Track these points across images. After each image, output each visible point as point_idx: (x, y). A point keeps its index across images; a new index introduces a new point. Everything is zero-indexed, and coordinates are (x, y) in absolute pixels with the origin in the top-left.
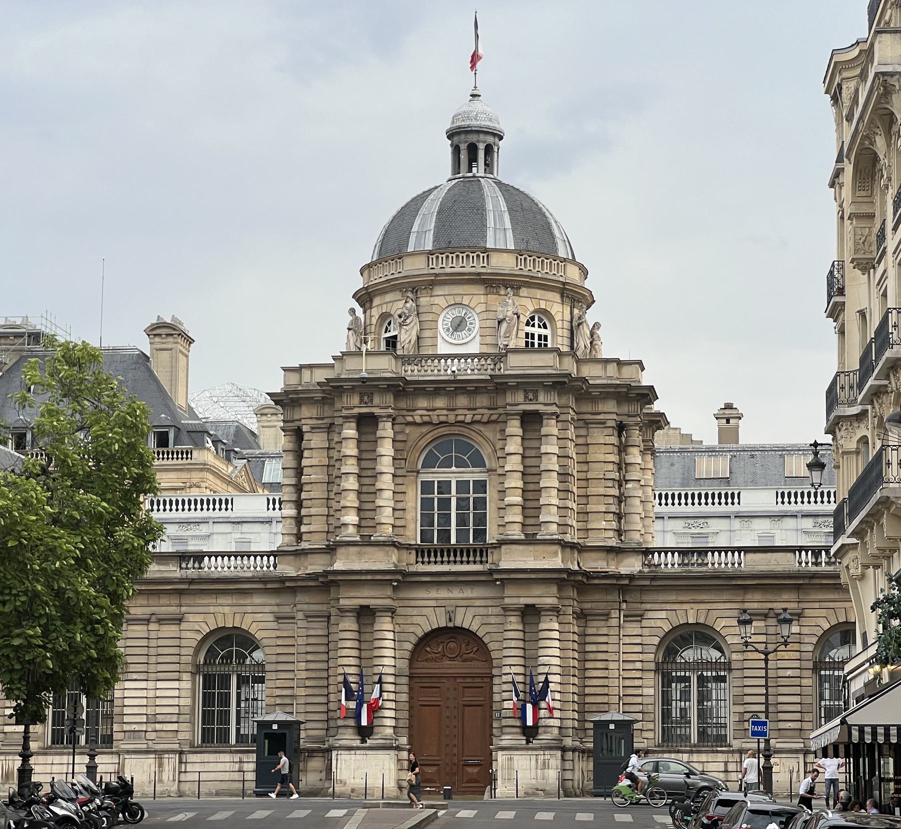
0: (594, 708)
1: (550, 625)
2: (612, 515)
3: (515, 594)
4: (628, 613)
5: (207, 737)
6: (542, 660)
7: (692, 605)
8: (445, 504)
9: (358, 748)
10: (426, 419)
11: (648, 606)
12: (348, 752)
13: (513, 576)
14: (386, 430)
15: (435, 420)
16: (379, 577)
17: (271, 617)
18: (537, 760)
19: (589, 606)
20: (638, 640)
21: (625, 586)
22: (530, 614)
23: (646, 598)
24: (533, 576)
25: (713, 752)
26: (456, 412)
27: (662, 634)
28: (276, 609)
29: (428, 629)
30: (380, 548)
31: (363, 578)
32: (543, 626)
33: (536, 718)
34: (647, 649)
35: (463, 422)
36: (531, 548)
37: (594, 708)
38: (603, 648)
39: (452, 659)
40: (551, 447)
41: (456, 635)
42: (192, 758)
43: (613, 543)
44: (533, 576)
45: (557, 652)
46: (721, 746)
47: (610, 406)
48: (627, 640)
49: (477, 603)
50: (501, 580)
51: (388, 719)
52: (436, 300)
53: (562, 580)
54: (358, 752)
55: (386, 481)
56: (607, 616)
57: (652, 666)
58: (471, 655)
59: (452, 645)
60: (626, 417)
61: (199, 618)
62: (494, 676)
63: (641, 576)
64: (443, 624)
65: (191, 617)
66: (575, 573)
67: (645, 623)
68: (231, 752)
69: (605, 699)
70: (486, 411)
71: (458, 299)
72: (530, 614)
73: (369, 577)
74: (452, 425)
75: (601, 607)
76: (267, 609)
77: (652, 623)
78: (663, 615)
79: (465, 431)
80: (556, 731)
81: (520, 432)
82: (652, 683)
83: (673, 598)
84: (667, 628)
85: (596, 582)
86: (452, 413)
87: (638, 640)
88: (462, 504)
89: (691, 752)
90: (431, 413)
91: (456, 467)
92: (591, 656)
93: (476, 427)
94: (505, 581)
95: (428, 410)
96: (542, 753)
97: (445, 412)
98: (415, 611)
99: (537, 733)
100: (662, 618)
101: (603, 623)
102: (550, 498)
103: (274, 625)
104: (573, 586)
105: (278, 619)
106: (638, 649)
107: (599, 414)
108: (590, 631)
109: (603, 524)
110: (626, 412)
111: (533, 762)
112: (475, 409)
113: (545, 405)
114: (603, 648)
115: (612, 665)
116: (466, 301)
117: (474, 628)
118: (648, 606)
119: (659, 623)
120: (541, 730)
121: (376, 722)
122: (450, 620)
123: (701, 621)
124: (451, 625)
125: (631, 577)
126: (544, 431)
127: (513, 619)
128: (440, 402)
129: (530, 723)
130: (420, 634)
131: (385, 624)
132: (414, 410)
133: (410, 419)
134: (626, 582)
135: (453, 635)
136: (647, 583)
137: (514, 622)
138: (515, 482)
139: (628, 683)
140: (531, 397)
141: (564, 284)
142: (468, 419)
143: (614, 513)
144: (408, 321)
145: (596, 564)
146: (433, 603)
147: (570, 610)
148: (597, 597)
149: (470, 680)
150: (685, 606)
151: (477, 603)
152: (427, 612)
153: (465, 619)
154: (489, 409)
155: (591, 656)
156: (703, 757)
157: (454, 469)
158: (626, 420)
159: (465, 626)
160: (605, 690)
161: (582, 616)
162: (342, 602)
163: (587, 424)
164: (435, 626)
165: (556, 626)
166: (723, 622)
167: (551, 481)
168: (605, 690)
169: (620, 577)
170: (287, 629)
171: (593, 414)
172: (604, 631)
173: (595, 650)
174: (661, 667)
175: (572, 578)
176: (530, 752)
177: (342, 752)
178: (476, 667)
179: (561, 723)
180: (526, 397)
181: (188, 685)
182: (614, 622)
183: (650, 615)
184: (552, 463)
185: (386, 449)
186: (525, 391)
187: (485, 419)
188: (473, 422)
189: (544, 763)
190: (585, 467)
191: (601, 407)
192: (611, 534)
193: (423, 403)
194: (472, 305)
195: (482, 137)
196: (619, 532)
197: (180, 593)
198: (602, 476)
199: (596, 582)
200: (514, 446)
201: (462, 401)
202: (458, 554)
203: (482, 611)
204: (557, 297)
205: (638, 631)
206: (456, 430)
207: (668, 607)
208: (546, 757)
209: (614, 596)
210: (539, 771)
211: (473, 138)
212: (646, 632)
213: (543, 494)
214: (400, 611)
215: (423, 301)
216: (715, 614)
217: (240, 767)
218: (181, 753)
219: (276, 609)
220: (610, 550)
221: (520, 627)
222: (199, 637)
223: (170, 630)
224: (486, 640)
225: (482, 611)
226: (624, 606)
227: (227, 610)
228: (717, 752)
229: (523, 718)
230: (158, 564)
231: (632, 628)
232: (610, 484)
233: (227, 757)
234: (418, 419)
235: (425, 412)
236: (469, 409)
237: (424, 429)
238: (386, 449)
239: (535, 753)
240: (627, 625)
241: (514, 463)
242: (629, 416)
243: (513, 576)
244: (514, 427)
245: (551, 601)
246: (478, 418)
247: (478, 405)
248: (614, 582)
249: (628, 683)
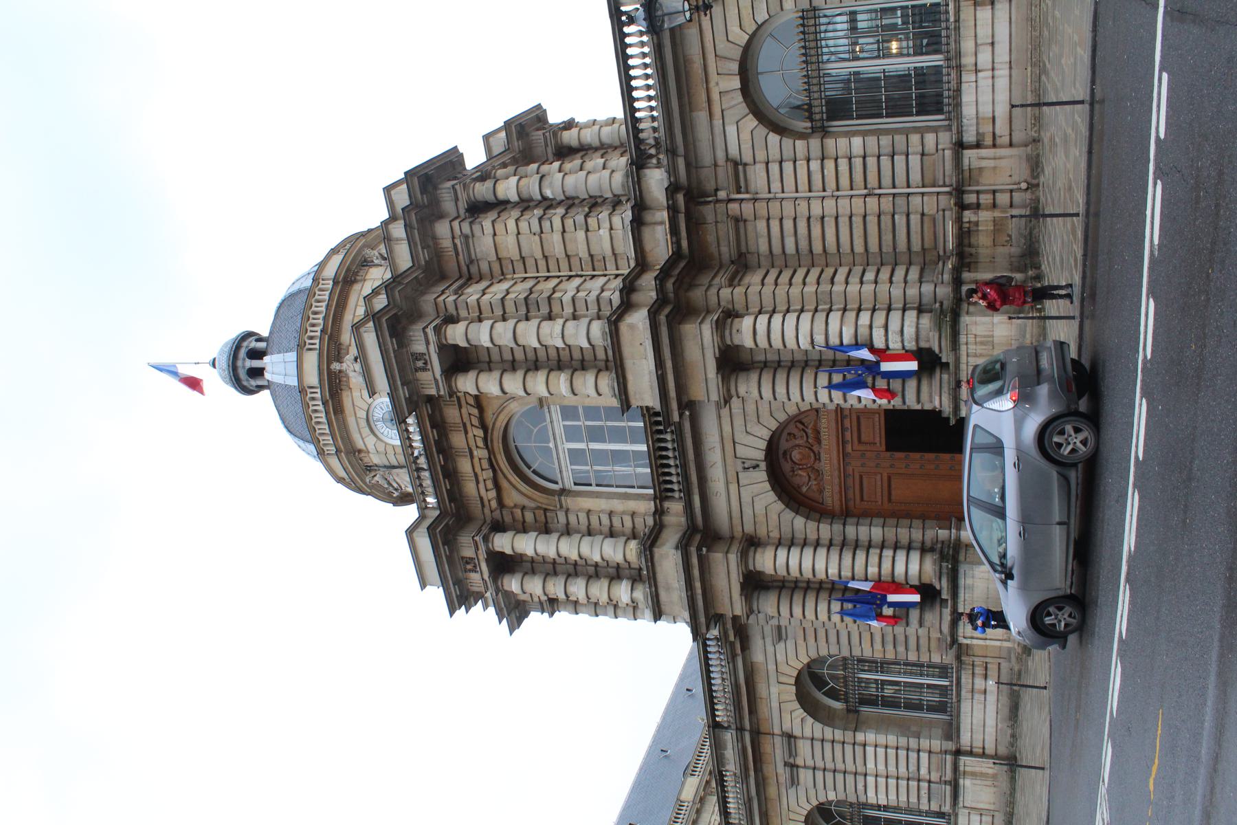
0: (887, 238)
1: (746, 332)
2: (589, 220)
3: (704, 385)
4: (733, 187)
5: (941, 708)
6: (804, 343)
7: (712, 84)
8: (600, 457)
10: (490, 484)
11: (721, 155)
13: (672, 393)
14: (503, 543)
15: (490, 473)
16: (696, 572)
17: (782, 644)
18: (976, 356)
19: (724, 249)
20: (774, 168)
21: (690, 197)
22: (733, 362)
23: (707, 159)
24: (669, 364)
25: (957, 29)
26: (474, 448)
27: (762, 131)
28: (769, 641)
29: (771, 496)
30: (657, 564)
31: (699, 591)
32: (748, 343)
33: (906, 356)
34: (788, 153)
35: (485, 439)
36: (628, 364)
37: (887, 238)
38: (788, 225)
39: (818, 458)
40: (482, 335)
41: (781, 452)
42: (965, 739)
43: (628, 215)
44: (669, 364)
45: (791, 318)
46: (947, 12)
47: (442, 229)
48: (776, 186)
49: (727, 428)
50: (681, 408)
51: (910, 566)
52: (371, 448)
53: (673, 312)
55: (569, 549)
56: (738, 220)
57: (815, 143)
58: (809, 431)
59: (796, 455)
60: (460, 204)
61: (786, 717)
63: (672, 171)
64: (761, 475)
65: (787, 727)
66: (661, 289)
67: (747, 158)
68: (959, 701)
69: (872, 220)
70: (464, 410)
71: (363, 423)
72: (733, 362)
73: (698, 585)
74: (491, 452)
75: (726, 229)
76: (770, 649)
77: (746, 147)
78: (731, 130)
79: (497, 435)
80: (926, 321)
81: (472, 375)
82: (842, 142)
83: (701, 117)
84: (751, 122)
85: (685, 244)
86: (475, 453)
87: (774, 168)
88: (595, 435)
89: (959, 68)
90: (481, 479)
91: (549, 442)
92: (803, 244)
93: (490, 423)
94: (685, 399)
95: (478, 482)
96: (963, 348)
97: (476, 460)
98: (748, 512)
99: (929, 351)
100: (733, 132)
101: (750, 227)
102: (553, 334)
103: (790, 644)
104: (688, 290)
105: (780, 638)
106: (788, 166)
107: (455, 245)
108: (764, 248)
109: (604, 232)
110: (453, 203)
112: (464, 425)
113: (428, 343)
114: (788, 225)
115: (816, 210)
116: (362, 414)
117: (766, 434)
118: (721, 155)
119: (746, 136)
120: (923, 345)
121: (915, 582)
122: (754, 467)
123: (735, 67)
124: (763, 465)
125: (672, 190)
126: (463, 344)
127: (742, 390)
128: (465, 466)
129: (913, 366)
130: (780, 506)
131: (767, 561)
132: (481, 499)
133: (494, 504)
134: (680, 198)
135: (781, 456)
136: (681, 162)
137: (747, 386)
138: (538, 383)
139: (845, 181)
140: (420, 364)
141: (335, 282)
142: (480, 433)
143: (587, 216)
144: (395, 485)
145: (659, 244)
146: (733, 488)
147: (725, 293)
148: (711, 238)
149: (848, 435)
150: (715, 96)
151: (727, 428)
152: (743, 497)
153: (754, 446)
154: (460, 407)
155: (803, 244)
156: (967, 45)
157: (551, 445)
158: (463, 205)
159: (763, 445)
160: (857, 221)
161: (742, 264)
162: (738, 612)
163: (472, 262)
164: (767, 486)
165: (747, 322)
166: (734, 29)
167: (529, 334)
168: (857, 221)
169: (673, 209)
170: (794, 629)
171: (457, 254)
172: (761, 225)
173: (793, 239)
174: (819, 124)
175: (671, 295)
179: (875, 547)
180: (424, 369)
181: (871, 737)
182: (747, 209)
183: (733, 151)
184: (504, 332)
185: (526, 545)
186: (416, 370)
187: (475, 411)
188: (484, 426)
189: (982, 343)
190: (530, 263)
191: (446, 243)
192: (617, 220)
193: (470, 488)
194: (366, 407)
195: (239, 363)
196: (616, 203)
197: (756, 734)
198: (537, 238)
199: (685, 244)
200: (489, 384)
201: (458, 440)
202: (663, 445)
203: (739, 422)
204: (357, 287)
205: (760, 167)
206: (498, 446)
207: (718, 122)
208: (971, 339)
209: (708, 211)
211: (242, 374)
212: (761, 156)
213: (549, 342)
214: (749, 528)
215: (375, 459)
216: (722, 46)
217: (979, 692)
218: (958, 753)
219: (769, 641)
220: (638, 223)
221: (754, 376)
222: (810, 720)
223: (804, 748)
224: (782, 417)
225: (739, 422)
226: (722, 194)
227: (774, 690)
228: (957, 20)
229: (904, 375)
230: (725, 749)
231: (757, 177)
232: (546, 224)
233: (965, 707)
234: (493, 494)
235: (481, 486)
236: (466, 433)
237: (504, 484)
238: (526, 545)
239: (963, 359)
240: (752, 188)
241: (513, 384)
242: (457, 199)
243: (672, 393)
244: (466, 383)
245: (707, 330)
246: (475, 421)
247: (458, 420)
248: (682, 218)
249: (845, 181)
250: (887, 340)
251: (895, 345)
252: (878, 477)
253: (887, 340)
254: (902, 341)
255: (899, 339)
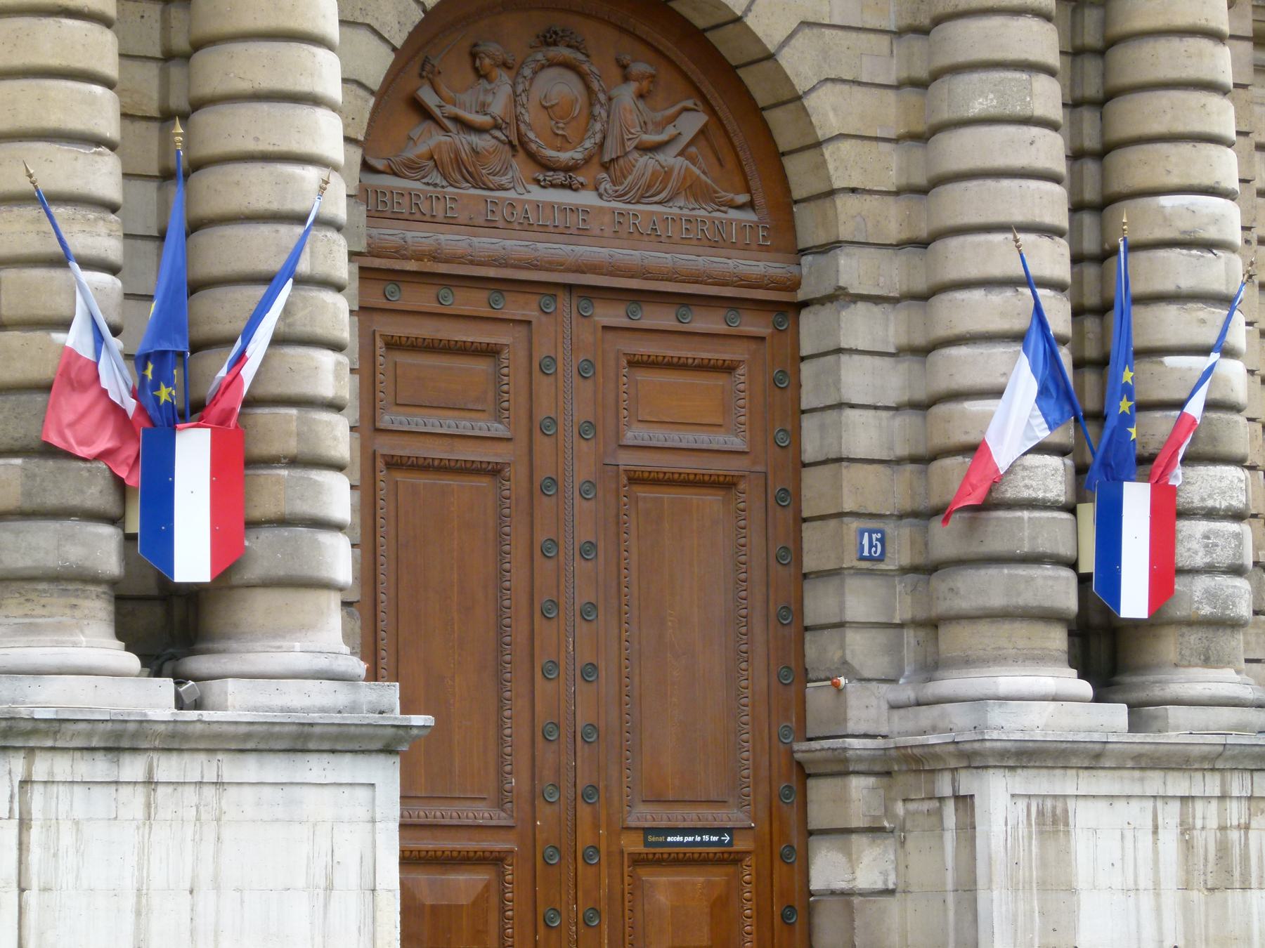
9: (175, 741)
12: (99, 768)
18: (1186, 828)
39: (564, 175)
54: (168, 768)
62: (840, 296)
96: (1212, 785)
111: (1170, 840)
176: (1154, 782)
177: (62, 767)
178: (707, 243)
189: (1223, 850)
208: (1235, 812)
210: (1197, 896)
224: (800, 64)
239: (1179, 785)
250: (1211, 514)
251: (1193, 540)
252: (485, 426)
253: (1211, 514)
254: (1210, 570)
255: (1223, 556)
